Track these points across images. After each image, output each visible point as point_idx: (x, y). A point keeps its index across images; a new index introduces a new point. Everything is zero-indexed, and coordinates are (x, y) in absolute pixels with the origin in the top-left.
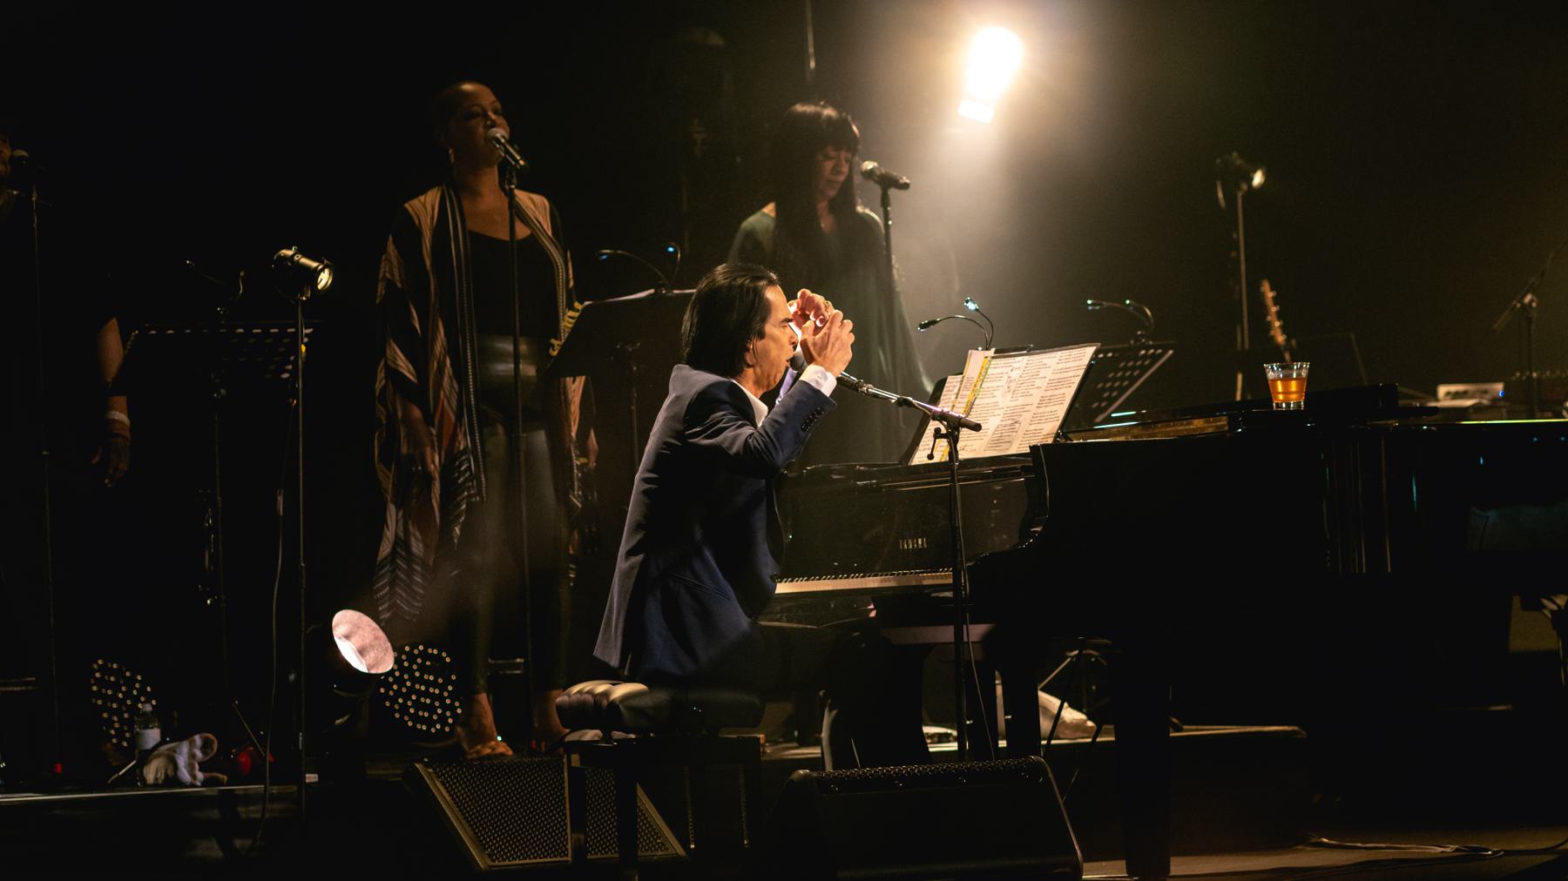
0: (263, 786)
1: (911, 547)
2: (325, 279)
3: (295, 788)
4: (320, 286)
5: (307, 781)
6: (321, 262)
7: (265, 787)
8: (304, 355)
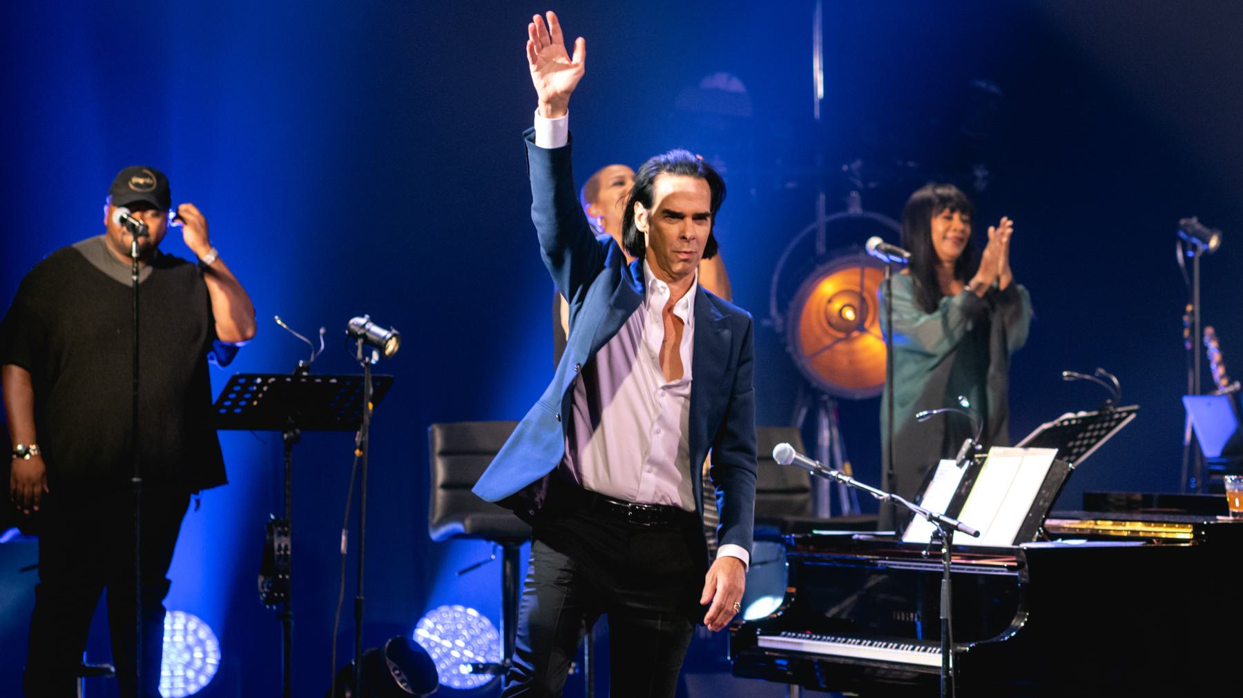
1: (903, 619)
2: (392, 346)
6: (389, 330)
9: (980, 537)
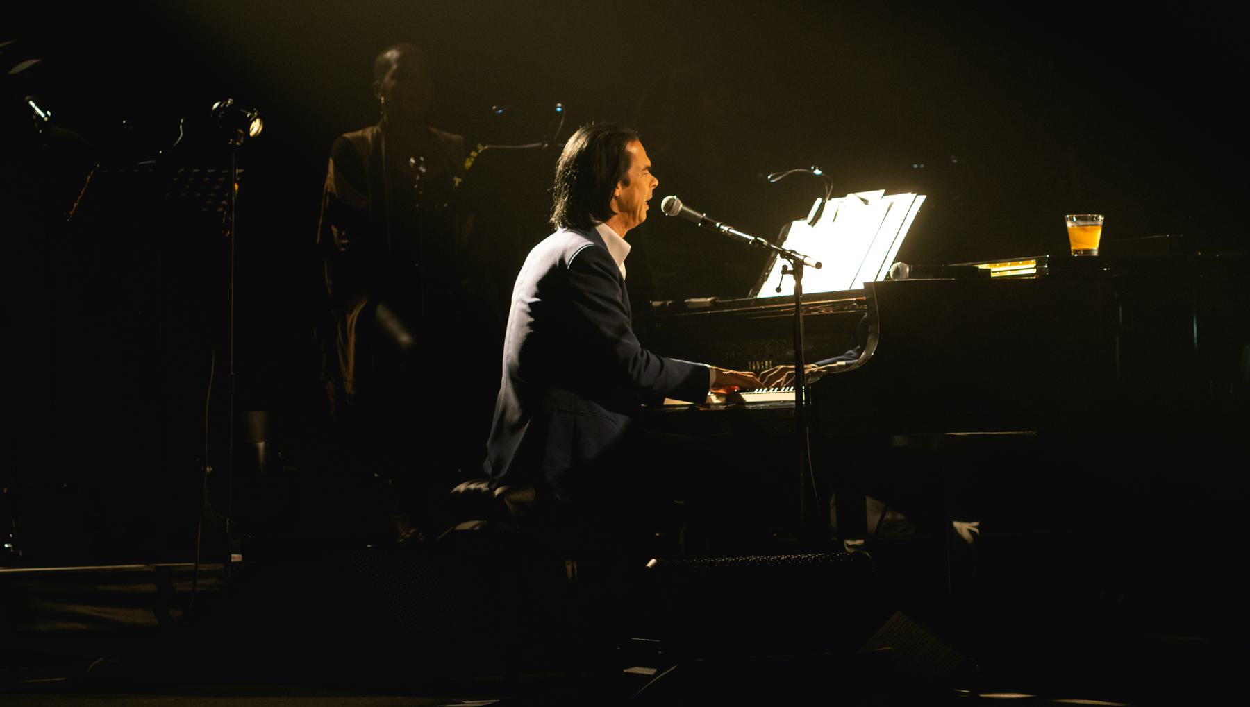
0: (194, 564)
3: (221, 566)
4: (252, 134)
5: (233, 560)
7: (196, 566)
8: (236, 192)
9: (821, 269)
